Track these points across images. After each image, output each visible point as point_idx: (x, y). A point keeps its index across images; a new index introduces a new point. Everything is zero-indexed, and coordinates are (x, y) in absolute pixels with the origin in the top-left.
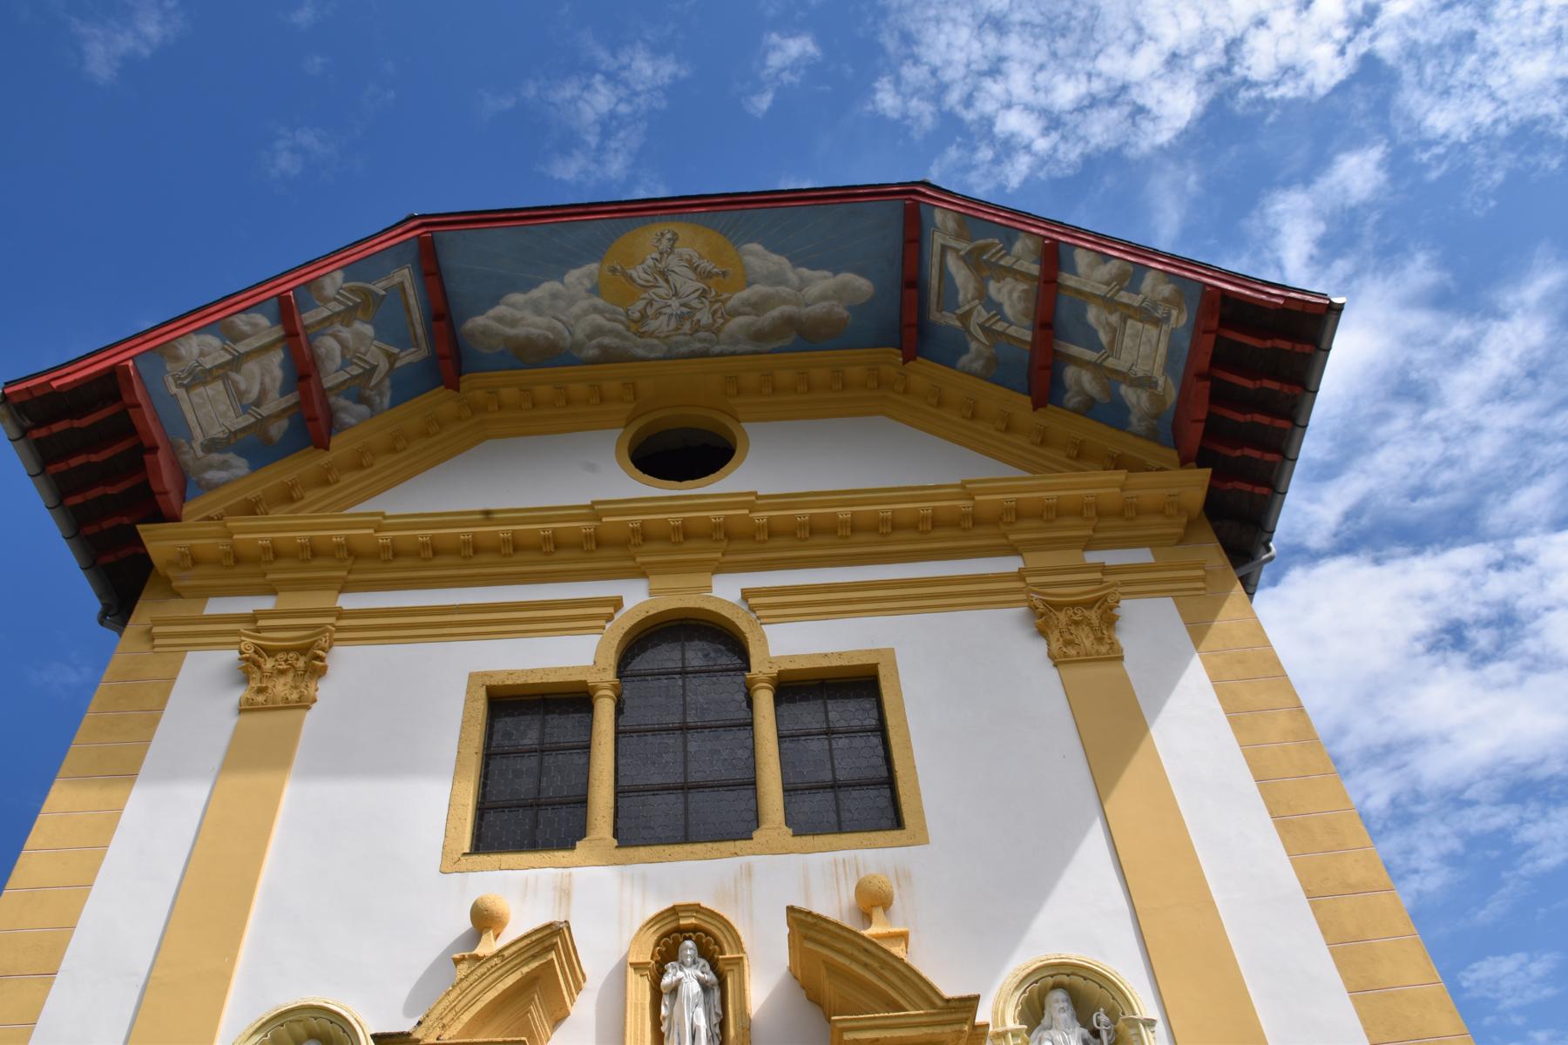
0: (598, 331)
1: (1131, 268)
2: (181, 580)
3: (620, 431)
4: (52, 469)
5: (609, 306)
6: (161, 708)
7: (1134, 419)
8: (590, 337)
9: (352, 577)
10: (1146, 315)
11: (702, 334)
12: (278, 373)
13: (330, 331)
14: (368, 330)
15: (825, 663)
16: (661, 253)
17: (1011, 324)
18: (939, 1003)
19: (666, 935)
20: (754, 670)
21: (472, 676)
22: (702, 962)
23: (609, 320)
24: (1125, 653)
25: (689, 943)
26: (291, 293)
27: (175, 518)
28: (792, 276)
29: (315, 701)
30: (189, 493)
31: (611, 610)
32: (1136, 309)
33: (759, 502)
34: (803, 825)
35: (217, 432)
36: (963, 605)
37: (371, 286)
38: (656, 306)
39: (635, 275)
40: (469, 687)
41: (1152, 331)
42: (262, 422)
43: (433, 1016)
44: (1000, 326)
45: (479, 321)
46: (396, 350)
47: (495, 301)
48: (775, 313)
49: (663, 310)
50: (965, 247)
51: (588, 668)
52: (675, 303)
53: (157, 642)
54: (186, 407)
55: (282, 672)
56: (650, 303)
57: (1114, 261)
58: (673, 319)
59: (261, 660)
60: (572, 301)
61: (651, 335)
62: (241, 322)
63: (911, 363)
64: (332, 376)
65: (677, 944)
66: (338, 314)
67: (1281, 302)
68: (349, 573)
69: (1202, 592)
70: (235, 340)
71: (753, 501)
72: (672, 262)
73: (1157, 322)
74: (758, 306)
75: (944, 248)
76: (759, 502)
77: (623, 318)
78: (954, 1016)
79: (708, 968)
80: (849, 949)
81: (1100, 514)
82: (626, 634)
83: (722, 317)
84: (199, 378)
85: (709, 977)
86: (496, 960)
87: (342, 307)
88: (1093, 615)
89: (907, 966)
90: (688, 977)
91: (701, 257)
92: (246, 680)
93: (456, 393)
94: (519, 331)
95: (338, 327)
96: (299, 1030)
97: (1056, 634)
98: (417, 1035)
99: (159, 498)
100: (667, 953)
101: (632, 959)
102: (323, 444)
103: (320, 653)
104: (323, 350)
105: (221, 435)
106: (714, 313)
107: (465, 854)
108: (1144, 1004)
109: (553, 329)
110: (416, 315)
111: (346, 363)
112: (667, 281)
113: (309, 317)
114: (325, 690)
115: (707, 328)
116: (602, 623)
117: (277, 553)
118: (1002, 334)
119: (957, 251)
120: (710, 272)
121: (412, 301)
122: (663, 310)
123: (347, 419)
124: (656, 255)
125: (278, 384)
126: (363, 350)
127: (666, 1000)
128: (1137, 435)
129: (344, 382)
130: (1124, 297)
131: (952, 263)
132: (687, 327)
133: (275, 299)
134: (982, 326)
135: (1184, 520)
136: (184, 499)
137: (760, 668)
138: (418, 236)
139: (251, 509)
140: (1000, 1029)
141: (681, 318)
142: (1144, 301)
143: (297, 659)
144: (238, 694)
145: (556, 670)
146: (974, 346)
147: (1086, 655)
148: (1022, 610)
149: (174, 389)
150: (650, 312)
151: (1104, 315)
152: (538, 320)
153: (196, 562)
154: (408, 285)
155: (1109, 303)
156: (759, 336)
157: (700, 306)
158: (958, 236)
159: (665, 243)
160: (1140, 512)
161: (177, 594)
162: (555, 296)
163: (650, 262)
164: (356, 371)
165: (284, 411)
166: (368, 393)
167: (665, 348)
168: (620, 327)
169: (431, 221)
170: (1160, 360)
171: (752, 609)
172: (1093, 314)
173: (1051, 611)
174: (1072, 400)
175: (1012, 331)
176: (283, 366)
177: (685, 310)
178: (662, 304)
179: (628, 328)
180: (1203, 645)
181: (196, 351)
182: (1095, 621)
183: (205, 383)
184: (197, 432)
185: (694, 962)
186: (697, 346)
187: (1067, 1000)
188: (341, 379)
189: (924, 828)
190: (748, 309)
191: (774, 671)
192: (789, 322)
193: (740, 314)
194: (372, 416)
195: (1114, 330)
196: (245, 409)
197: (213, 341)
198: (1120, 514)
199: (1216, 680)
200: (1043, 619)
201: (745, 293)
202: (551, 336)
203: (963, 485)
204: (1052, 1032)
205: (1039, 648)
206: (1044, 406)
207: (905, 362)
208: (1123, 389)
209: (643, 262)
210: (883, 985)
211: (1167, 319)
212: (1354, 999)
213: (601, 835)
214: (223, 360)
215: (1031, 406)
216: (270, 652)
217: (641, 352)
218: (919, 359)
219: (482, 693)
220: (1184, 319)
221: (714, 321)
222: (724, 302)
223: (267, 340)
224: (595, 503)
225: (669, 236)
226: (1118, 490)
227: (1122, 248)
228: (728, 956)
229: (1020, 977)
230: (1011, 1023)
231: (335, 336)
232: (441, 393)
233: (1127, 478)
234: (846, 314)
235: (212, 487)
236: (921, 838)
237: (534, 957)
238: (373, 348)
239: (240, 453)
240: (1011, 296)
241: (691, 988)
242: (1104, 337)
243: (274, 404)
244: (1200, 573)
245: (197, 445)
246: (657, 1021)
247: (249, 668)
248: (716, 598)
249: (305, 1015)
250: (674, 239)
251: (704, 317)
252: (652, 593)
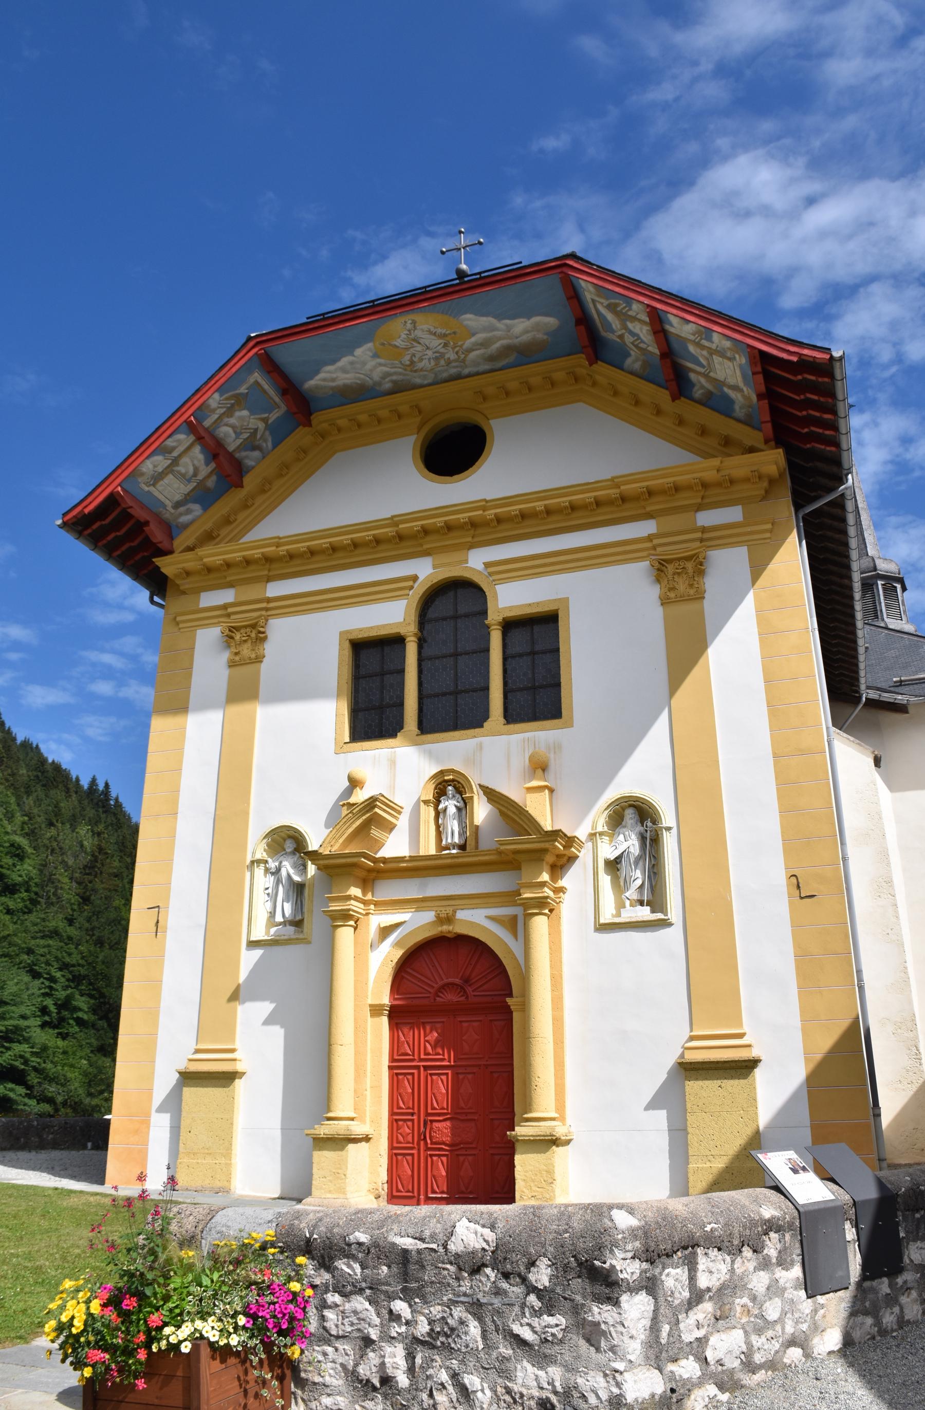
0: (386, 375)
1: (703, 329)
2: (185, 584)
3: (415, 436)
4: (100, 544)
5: (388, 362)
6: (190, 667)
7: (737, 407)
8: (383, 378)
9: (271, 573)
10: (721, 353)
11: (454, 364)
12: (201, 457)
13: (222, 424)
14: (245, 413)
15: (529, 611)
16: (409, 331)
17: (648, 346)
18: (543, 833)
19: (440, 784)
20: (490, 618)
21: (341, 633)
22: (458, 796)
23: (391, 368)
24: (706, 595)
25: (450, 788)
26: (192, 418)
27: (171, 552)
28: (501, 325)
29: (264, 657)
30: (174, 534)
31: (411, 583)
32: (714, 350)
33: (489, 504)
34: (512, 716)
35: (178, 497)
36: (614, 561)
37: (238, 392)
38: (418, 356)
39: (397, 344)
40: (340, 641)
41: (730, 364)
42: (201, 483)
43: (326, 842)
44: (642, 345)
45: (312, 383)
46: (266, 415)
47: (317, 372)
48: (498, 345)
49: (424, 357)
50: (606, 303)
51: (400, 623)
52: (429, 353)
53: (181, 626)
54: (156, 494)
55: (245, 641)
56: (414, 355)
57: (691, 325)
58: (432, 361)
59: (233, 634)
60: (364, 364)
61: (422, 370)
62: (170, 443)
63: (594, 365)
64: (232, 444)
65: (445, 788)
66: (224, 413)
67: (795, 359)
68: (269, 571)
69: (768, 541)
70: (170, 453)
71: (485, 505)
72: (418, 333)
73: (730, 359)
74: (485, 344)
75: (593, 301)
76: (489, 504)
77: (400, 366)
78: (550, 838)
79: (460, 799)
80: (506, 805)
81: (705, 485)
82: (421, 598)
83: (463, 353)
84: (157, 478)
85: (461, 804)
86: (350, 815)
87: (225, 409)
88: (690, 566)
89: (529, 814)
90: (450, 805)
91: (435, 328)
92: (228, 646)
93: (310, 429)
94: (339, 383)
95: (226, 420)
96: (283, 834)
97: (666, 581)
98: (320, 851)
99: (159, 545)
100: (440, 793)
101: (423, 798)
102: (240, 485)
103: (261, 629)
104: (222, 434)
105: (181, 498)
106: (457, 353)
107: (345, 743)
108: (668, 818)
109: (359, 379)
110: (272, 392)
111: (238, 434)
112: (420, 343)
113: (207, 423)
114: (269, 648)
115: (456, 361)
116: (406, 592)
117: (228, 565)
118: (645, 350)
119: (602, 304)
120: (444, 334)
121: (266, 387)
122: (424, 357)
123: (250, 463)
124: (408, 333)
125: (203, 462)
126: (245, 424)
127: (441, 816)
128: (738, 420)
129: (241, 444)
130: (705, 343)
132: (442, 362)
133: (184, 424)
134: (632, 343)
135: (765, 484)
136: (171, 538)
137: (494, 617)
138: (256, 353)
139: (209, 537)
140: (593, 832)
141: (436, 359)
142: (717, 347)
143: (251, 632)
144: (226, 656)
145: (384, 626)
146: (632, 353)
147: (681, 597)
148: (644, 566)
149: (146, 489)
150: (415, 359)
151: (699, 350)
152: (348, 376)
153: (188, 573)
154: (260, 380)
155: (698, 345)
156: (491, 358)
157: (446, 351)
158: (599, 296)
159: (409, 326)
160: (732, 482)
161: (184, 593)
162: (352, 363)
163: (404, 336)
164: (245, 436)
165: (211, 473)
166: (257, 443)
167: (433, 375)
168: (400, 370)
169: (261, 340)
170: (740, 379)
171: (490, 574)
172: (692, 348)
173: (663, 565)
174: (698, 393)
175: (650, 348)
176: (202, 452)
177: (438, 355)
178: (421, 354)
179: (405, 370)
180: (761, 582)
181: (151, 466)
182: (690, 571)
183: (162, 479)
184: (167, 502)
185: (454, 796)
186: (453, 371)
187: (635, 813)
188: (238, 443)
189: (571, 718)
190: (478, 347)
191: (500, 619)
192: (508, 350)
193: (473, 350)
194: (264, 457)
195: (707, 359)
196: (189, 481)
197: (158, 458)
198: (719, 484)
199: (759, 611)
200: (660, 570)
201: (473, 339)
202: (359, 382)
203: (612, 479)
204: (624, 830)
205: (653, 592)
206: (679, 398)
207: (591, 365)
208: (726, 389)
209: (400, 337)
210: (521, 822)
211: (734, 358)
212: (781, 817)
213: (410, 728)
214: (166, 465)
215: (670, 398)
216: (237, 629)
217: (418, 381)
219: (347, 645)
220: (744, 361)
221: (459, 357)
222: (461, 346)
223: (188, 444)
224: (393, 517)
225: (410, 322)
226: (715, 472)
227: (697, 312)
228: (467, 795)
229: (608, 804)
230: (601, 826)
231: (226, 425)
232: (302, 431)
233: (721, 462)
234: (545, 337)
235: (185, 526)
236: (570, 724)
237: (367, 812)
238: (251, 420)
239: (196, 501)
240: (643, 332)
241: (452, 810)
243: (204, 471)
245: (169, 508)
246: (438, 826)
247: (229, 637)
248: (471, 568)
249: (284, 830)
250: (414, 322)
251: (451, 355)
252: (434, 567)
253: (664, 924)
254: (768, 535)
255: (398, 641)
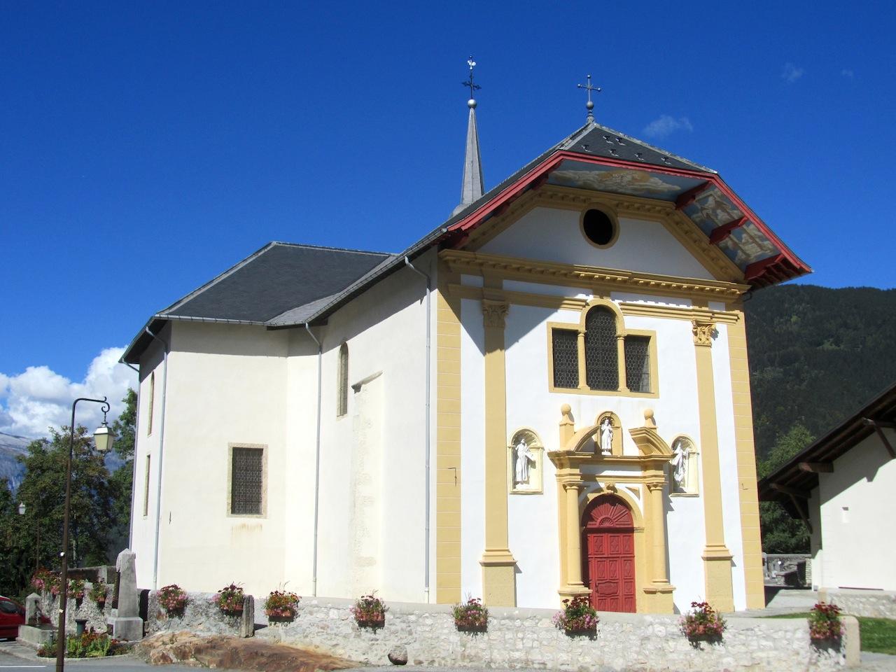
75: (711, 195)
116: (581, 307)
131: (711, 199)
172: (744, 235)
186: (615, 188)
207: (676, 209)
218: (681, 211)
220: (770, 254)
242: (743, 241)
244: (736, 318)
253: (696, 496)
254: (735, 321)
255: (574, 334)
